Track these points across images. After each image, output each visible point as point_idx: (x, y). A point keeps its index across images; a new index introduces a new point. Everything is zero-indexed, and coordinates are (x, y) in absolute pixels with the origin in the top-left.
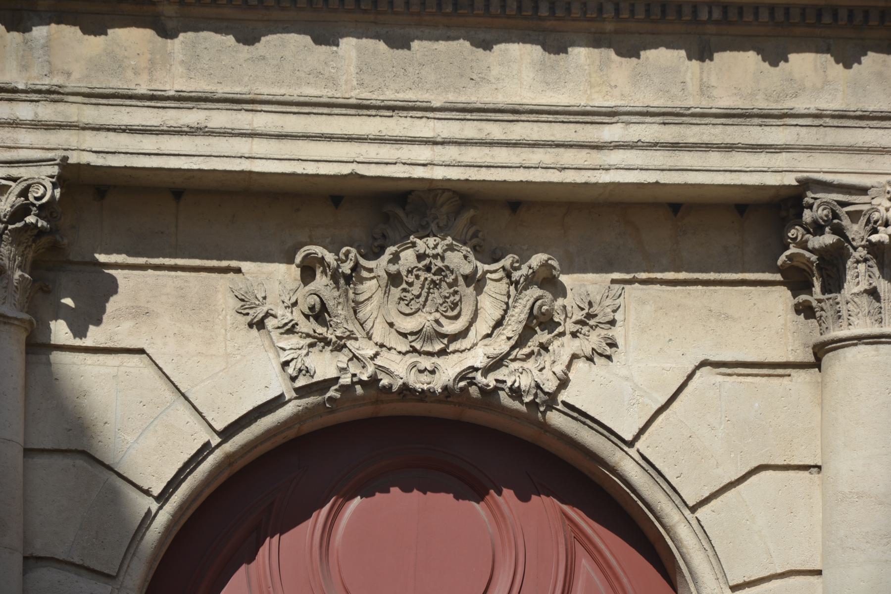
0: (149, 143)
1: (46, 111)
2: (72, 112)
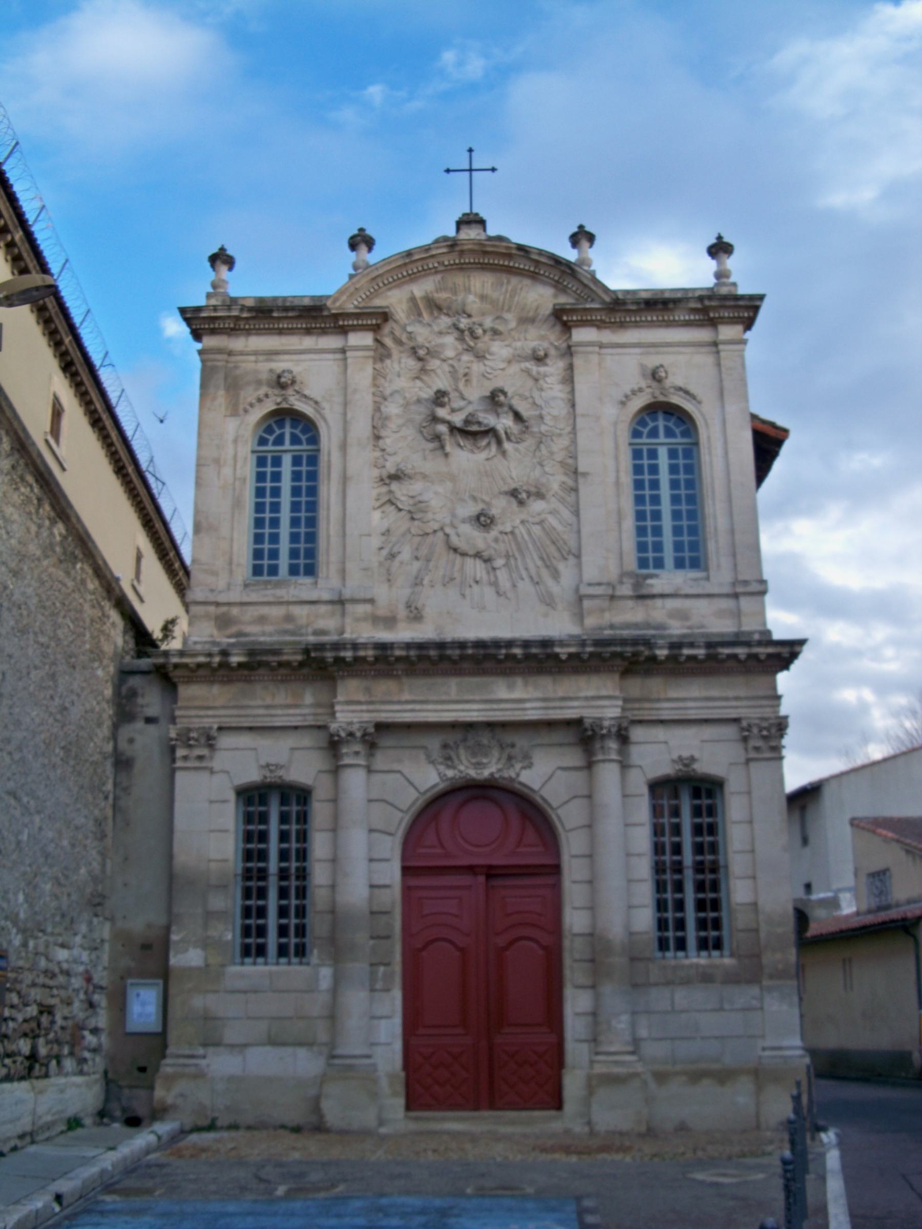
0: (398, 715)
1: (371, 707)
2: (378, 707)
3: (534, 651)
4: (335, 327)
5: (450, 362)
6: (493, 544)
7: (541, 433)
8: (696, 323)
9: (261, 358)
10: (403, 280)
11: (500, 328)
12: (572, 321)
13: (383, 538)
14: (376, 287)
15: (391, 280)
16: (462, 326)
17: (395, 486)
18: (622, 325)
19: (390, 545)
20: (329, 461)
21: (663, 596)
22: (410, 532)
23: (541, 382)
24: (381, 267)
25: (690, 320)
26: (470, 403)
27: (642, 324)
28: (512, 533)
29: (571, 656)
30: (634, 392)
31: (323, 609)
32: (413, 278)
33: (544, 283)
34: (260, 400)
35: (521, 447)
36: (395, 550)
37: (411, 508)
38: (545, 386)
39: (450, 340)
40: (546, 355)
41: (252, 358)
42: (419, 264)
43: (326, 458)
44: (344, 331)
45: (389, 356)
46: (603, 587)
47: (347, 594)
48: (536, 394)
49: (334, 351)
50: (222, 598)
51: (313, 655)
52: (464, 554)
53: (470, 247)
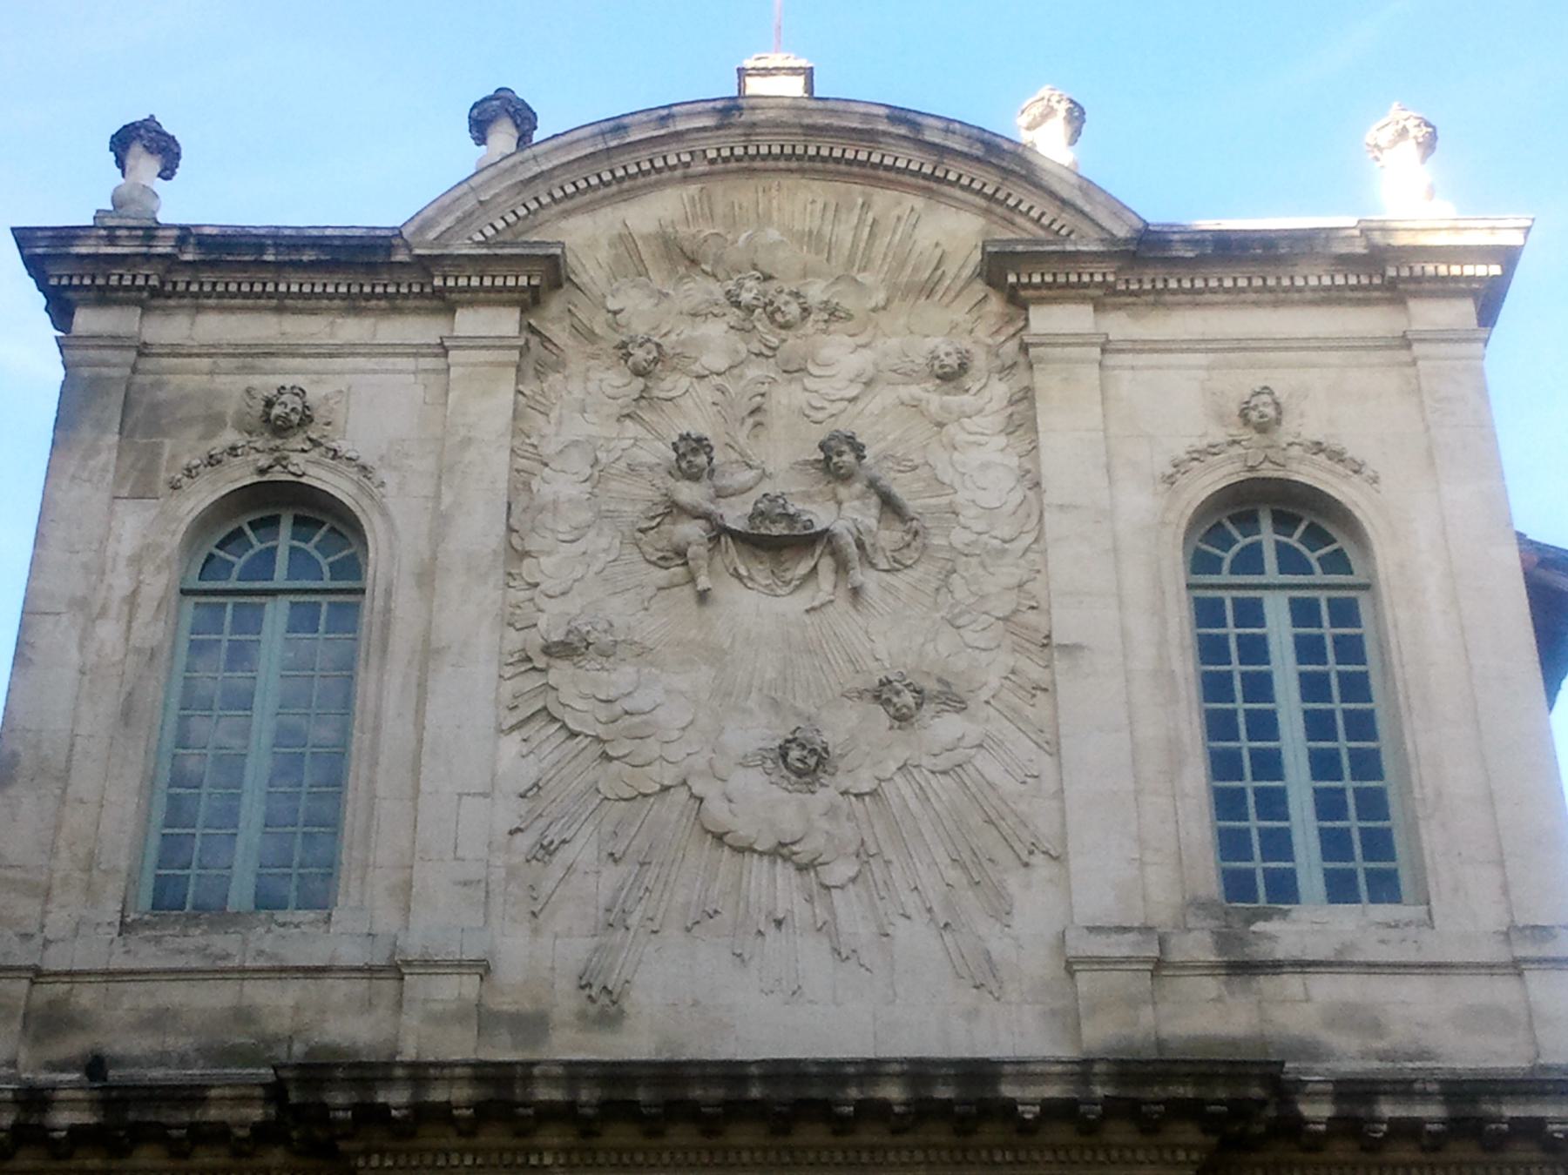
3: (943, 1092)
4: (421, 294)
5: (717, 380)
6: (824, 824)
7: (952, 547)
8: (1349, 294)
9: (224, 363)
10: (603, 191)
11: (848, 303)
12: (1030, 285)
13: (524, 805)
14: (533, 206)
15: (570, 189)
16: (746, 297)
17: (561, 672)
18: (1159, 300)
19: (541, 823)
20: (387, 610)
21: (1302, 966)
22: (598, 791)
23: (952, 429)
24: (546, 154)
25: (1333, 287)
26: (764, 475)
27: (1208, 297)
28: (873, 793)
29: (1051, 1109)
30: (1197, 455)
31: (339, 990)
32: (628, 187)
33: (962, 205)
34: (213, 461)
35: (899, 580)
36: (554, 835)
37: (600, 730)
38: (961, 437)
39: (715, 329)
40: (963, 368)
41: (205, 363)
42: (643, 155)
43: (379, 603)
44: (445, 303)
45: (559, 365)
46: (1131, 937)
47: (413, 946)
48: (939, 458)
49: (416, 351)
50: (54, 961)
51: (294, 1097)
52: (740, 850)
53: (771, 114)
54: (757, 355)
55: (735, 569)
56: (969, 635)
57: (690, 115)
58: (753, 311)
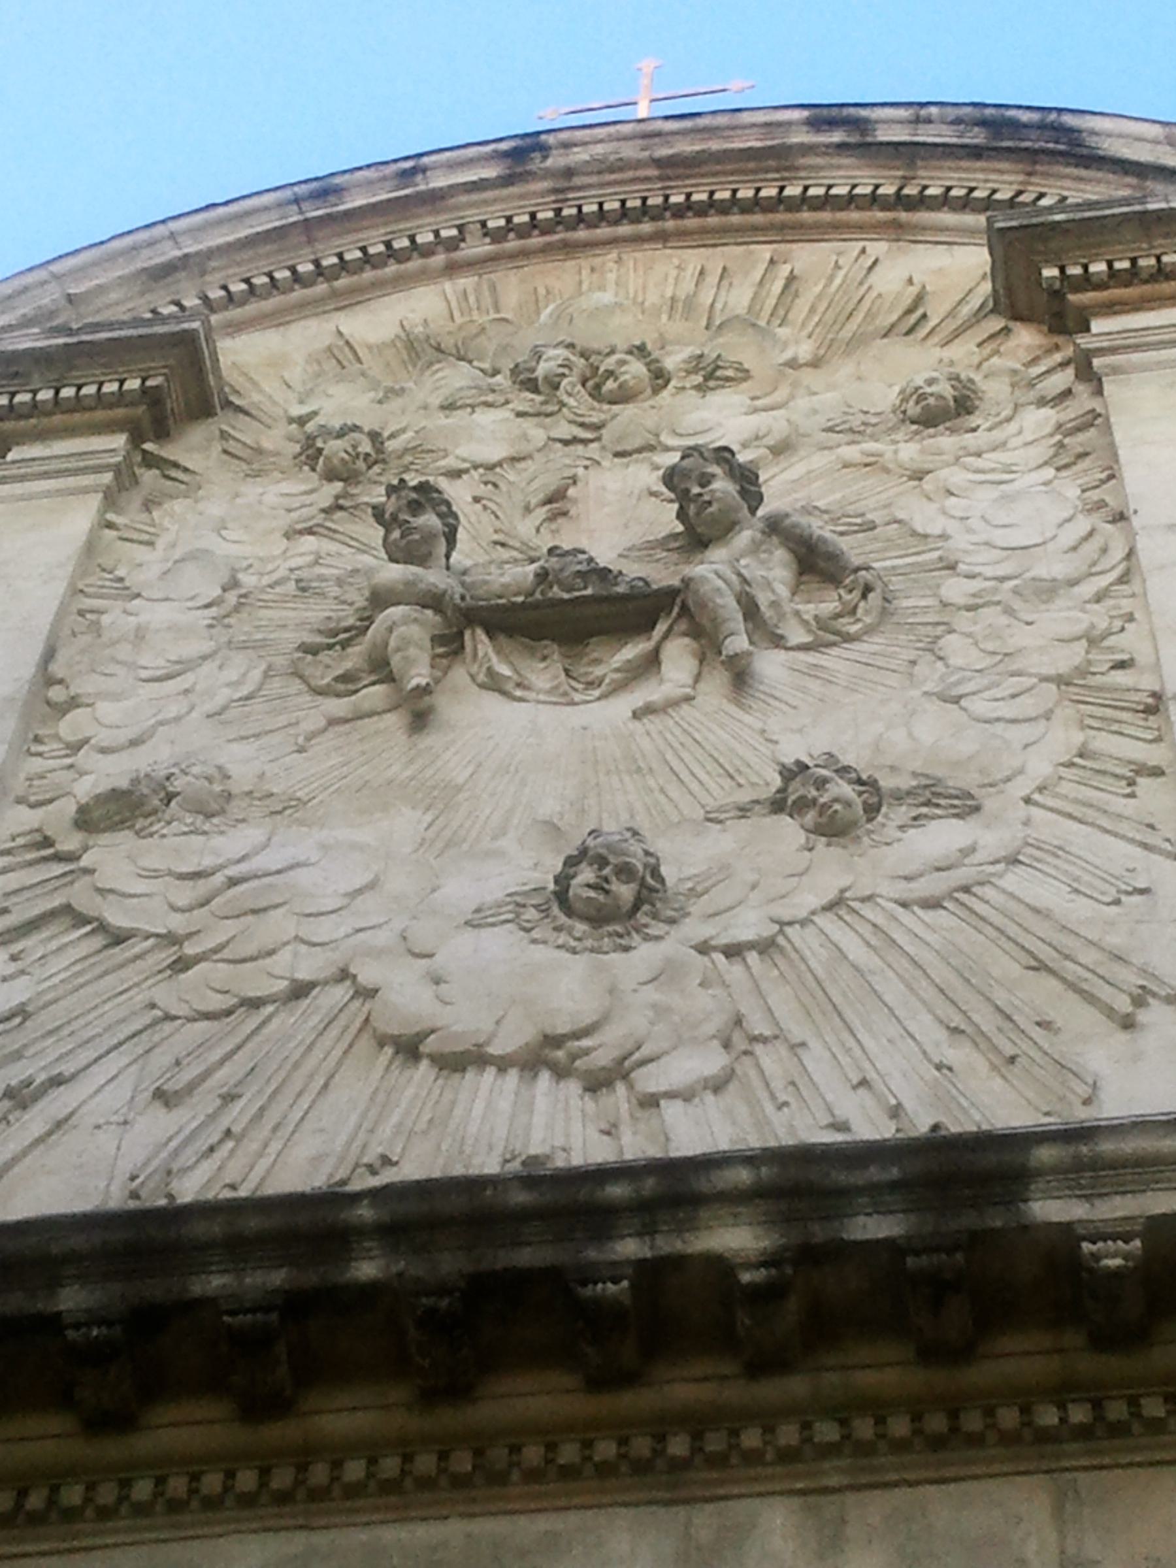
54: (566, 443)
55: (490, 672)
56: (979, 706)
57: (452, 166)
58: (557, 387)
